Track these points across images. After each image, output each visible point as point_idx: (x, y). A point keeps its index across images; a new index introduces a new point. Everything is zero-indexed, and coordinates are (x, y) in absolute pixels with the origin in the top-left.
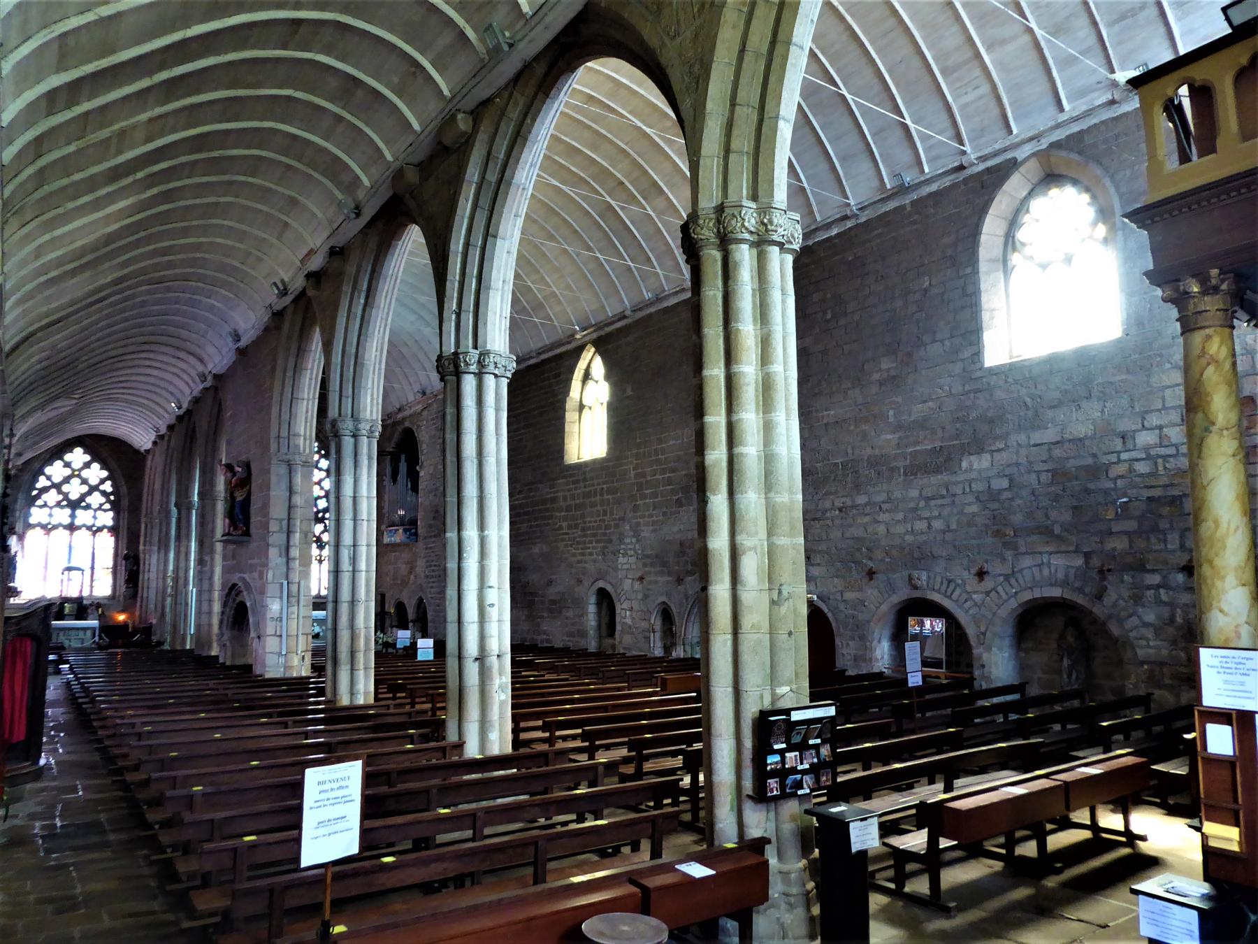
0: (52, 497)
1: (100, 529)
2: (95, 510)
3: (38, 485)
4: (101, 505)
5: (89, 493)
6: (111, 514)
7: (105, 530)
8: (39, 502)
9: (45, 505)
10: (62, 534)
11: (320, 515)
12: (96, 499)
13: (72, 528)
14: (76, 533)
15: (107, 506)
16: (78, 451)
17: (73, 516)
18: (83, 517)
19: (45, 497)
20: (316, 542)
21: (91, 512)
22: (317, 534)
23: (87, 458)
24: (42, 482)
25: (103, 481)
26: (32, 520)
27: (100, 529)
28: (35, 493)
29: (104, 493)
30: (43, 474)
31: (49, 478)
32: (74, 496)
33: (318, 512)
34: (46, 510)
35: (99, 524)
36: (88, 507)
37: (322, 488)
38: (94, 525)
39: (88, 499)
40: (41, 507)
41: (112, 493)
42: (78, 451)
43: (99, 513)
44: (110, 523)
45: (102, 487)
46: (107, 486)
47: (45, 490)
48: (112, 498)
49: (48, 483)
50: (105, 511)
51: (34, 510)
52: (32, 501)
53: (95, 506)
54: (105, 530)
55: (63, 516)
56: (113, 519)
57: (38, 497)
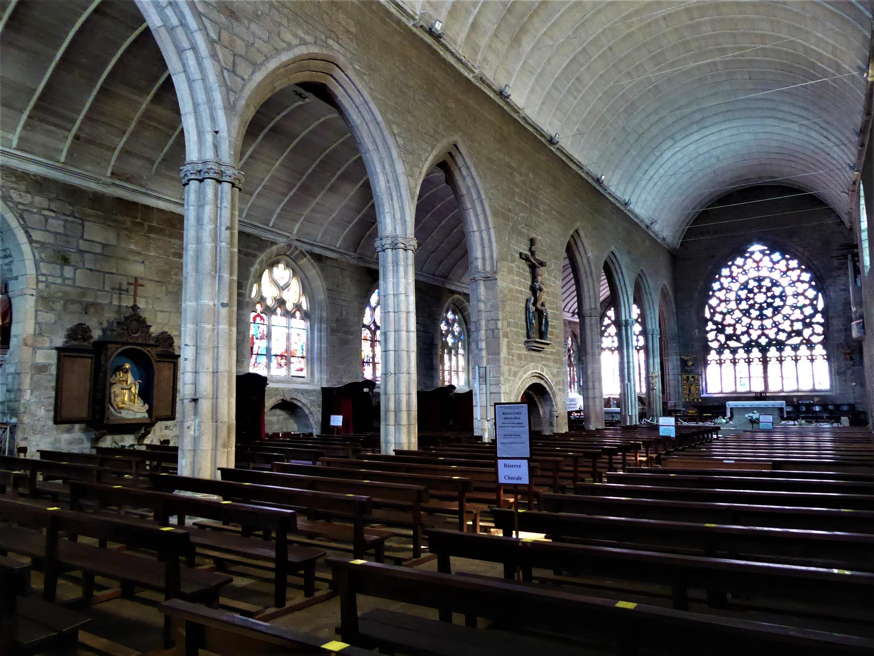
3: (605, 323)
8: (606, 334)
9: (610, 335)
11: (808, 321)
19: (609, 330)
20: (806, 344)
22: (807, 337)
26: (603, 346)
28: (603, 328)
30: (606, 316)
31: (609, 318)
33: (806, 317)
34: (610, 339)
37: (806, 297)
40: (607, 337)
47: (608, 326)
49: (610, 322)
51: (604, 339)
52: (602, 333)
57: (605, 331)
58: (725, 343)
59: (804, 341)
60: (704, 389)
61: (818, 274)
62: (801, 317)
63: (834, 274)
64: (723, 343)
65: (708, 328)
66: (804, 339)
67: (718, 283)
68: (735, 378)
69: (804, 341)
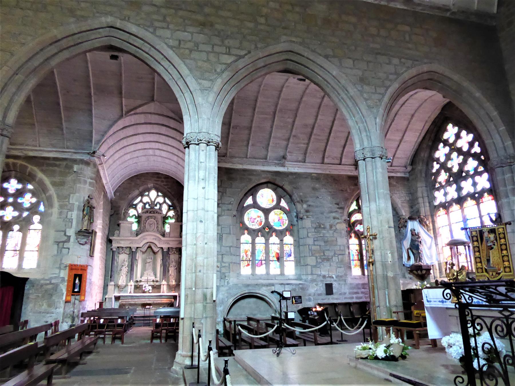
0: (443, 177)
1: (481, 194)
2: (473, 177)
4: (476, 169)
5: (465, 162)
6: (486, 176)
7: (486, 195)
8: (437, 185)
10: (455, 207)
12: (472, 164)
13: (460, 201)
14: (465, 205)
15: (481, 169)
16: (450, 126)
17: (459, 189)
18: (467, 186)
21: (470, 181)
23: (456, 129)
24: (436, 166)
25: (471, 145)
27: (481, 194)
29: (476, 156)
32: (455, 169)
35: (479, 188)
36: (468, 175)
38: (475, 193)
39: (466, 168)
41: (481, 153)
42: (450, 126)
43: (477, 178)
44: (488, 185)
45: (473, 151)
46: (477, 149)
47: (438, 172)
48: (482, 157)
50: (480, 174)
53: (472, 172)
54: (486, 195)
55: (452, 192)
56: (489, 180)
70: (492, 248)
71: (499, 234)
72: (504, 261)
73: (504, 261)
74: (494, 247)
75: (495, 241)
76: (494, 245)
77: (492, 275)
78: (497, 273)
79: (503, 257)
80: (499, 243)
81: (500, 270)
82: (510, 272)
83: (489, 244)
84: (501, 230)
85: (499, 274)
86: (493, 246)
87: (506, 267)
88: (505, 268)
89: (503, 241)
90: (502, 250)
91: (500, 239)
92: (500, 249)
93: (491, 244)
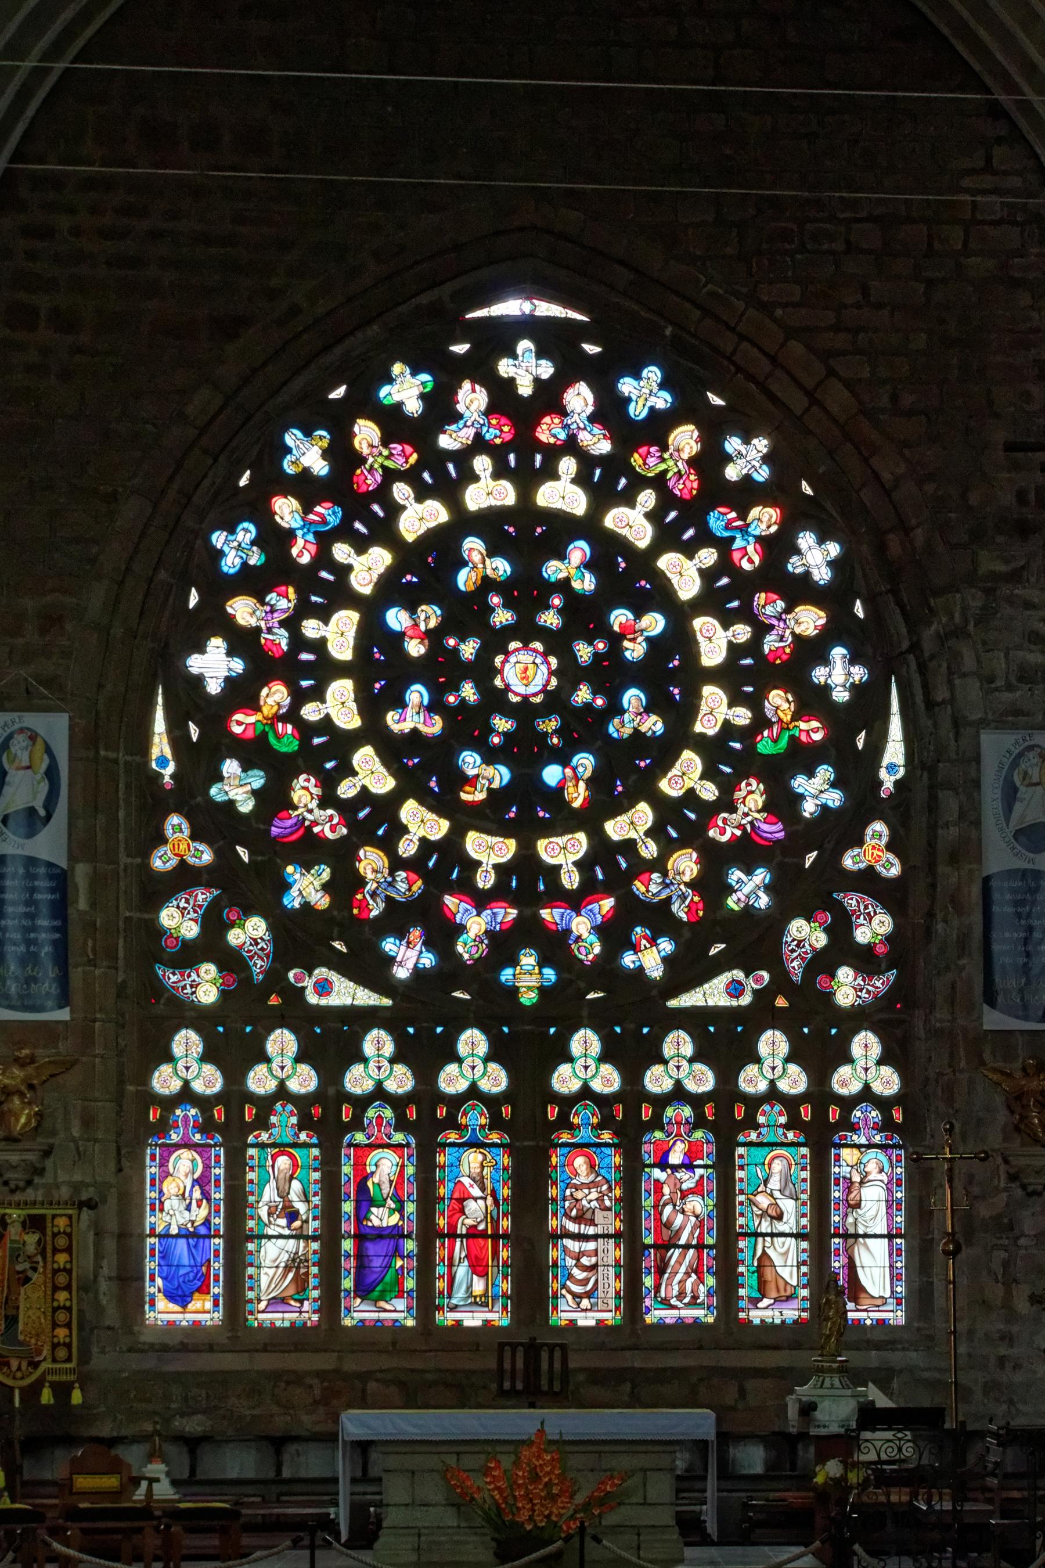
22: (796, 967)
58: (275, 978)
59: (781, 1002)
60: (112, 1316)
61: (894, 544)
62: (774, 831)
63: (990, 563)
64: (258, 967)
65: (162, 861)
66: (781, 982)
67: (247, 532)
68: (330, 1236)
69: (781, 1002)
70: (27, 1280)
71: (55, 1235)
72: (55, 1325)
73: (55, 1325)
74: (35, 1277)
75: (39, 1258)
76: (35, 1269)
77: (19, 1369)
78: (30, 1364)
79: (55, 1310)
80: (49, 1267)
81: (39, 1352)
82: (69, 1360)
83: (19, 1267)
84: (62, 1223)
85: (35, 1365)
86: (30, 1273)
87: (59, 1344)
88: (55, 1346)
89: (62, 1258)
90: (55, 1289)
91: (56, 1251)
92: (49, 1285)
93: (27, 1265)
